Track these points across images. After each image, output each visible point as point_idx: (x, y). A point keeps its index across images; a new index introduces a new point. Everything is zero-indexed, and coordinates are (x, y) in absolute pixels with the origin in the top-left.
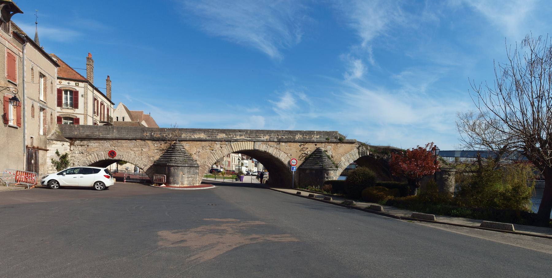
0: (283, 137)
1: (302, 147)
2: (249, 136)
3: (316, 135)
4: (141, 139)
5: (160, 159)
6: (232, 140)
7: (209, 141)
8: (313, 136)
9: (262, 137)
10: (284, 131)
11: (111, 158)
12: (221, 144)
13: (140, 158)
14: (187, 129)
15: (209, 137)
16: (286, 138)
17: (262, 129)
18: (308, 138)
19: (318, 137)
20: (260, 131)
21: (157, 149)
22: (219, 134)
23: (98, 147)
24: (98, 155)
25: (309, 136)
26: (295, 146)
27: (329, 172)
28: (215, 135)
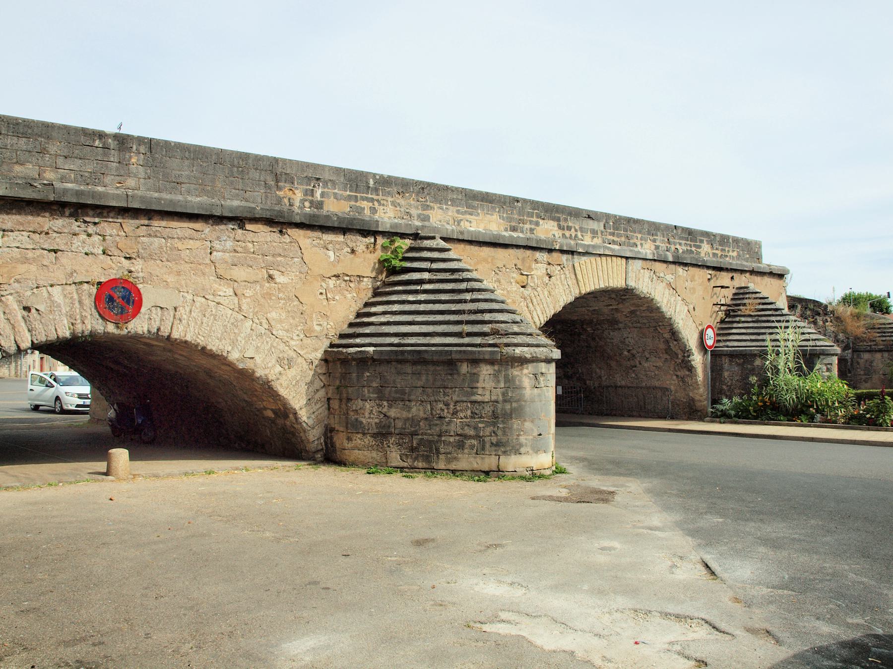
0: (678, 246)
1: (713, 283)
2: (611, 238)
4: (269, 222)
5: (351, 325)
6: (580, 250)
7: (518, 247)
9: (638, 244)
11: (111, 328)
12: (549, 264)
13: (264, 321)
14: (446, 188)
15: (514, 229)
17: (639, 218)
20: (636, 221)
21: (337, 276)
22: (541, 222)
23: (30, 254)
24: (27, 309)
25: (722, 250)
28: (531, 222)
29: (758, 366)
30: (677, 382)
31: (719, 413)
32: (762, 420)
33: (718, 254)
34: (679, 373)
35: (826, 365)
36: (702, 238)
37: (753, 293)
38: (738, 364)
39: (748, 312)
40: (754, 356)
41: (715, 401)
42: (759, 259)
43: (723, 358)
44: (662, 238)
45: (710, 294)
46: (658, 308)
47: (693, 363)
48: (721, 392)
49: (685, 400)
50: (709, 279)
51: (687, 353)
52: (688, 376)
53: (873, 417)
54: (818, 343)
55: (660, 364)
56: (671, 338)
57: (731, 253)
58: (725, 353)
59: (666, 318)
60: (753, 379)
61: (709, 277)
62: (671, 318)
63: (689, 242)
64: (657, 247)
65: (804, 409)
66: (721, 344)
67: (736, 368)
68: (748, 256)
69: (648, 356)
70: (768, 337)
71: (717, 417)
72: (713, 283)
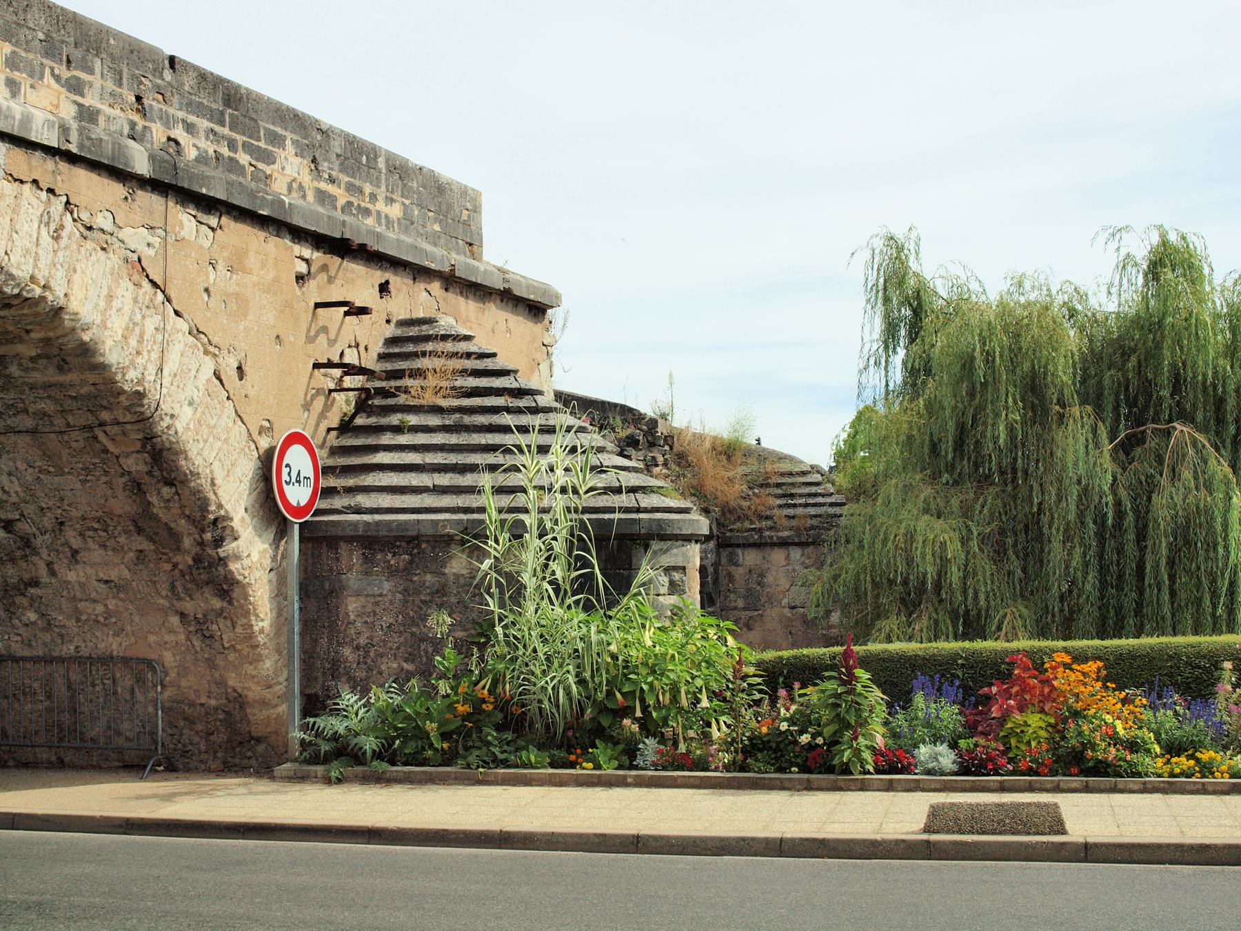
0: (179, 133)
1: (315, 291)
3: (383, 188)
10: (187, 66)
19: (395, 211)
25: (350, 188)
29: (457, 576)
30: (182, 637)
31: (325, 747)
32: (468, 766)
34: (188, 606)
35: (668, 570)
36: (279, 130)
37: (445, 338)
38: (392, 572)
39: (429, 399)
40: (443, 541)
41: (314, 704)
42: (473, 246)
43: (344, 549)
44: (110, 85)
45: (304, 326)
46: (86, 351)
47: (234, 567)
48: (335, 669)
49: (213, 702)
50: (300, 278)
51: (220, 529)
52: (220, 613)
53: (820, 741)
54: (646, 501)
55: (119, 572)
56: (150, 473)
57: (380, 206)
58: (349, 532)
59: (121, 392)
60: (441, 622)
61: (302, 268)
62: (140, 395)
63: (226, 131)
64: (88, 115)
65: (605, 723)
66: (338, 502)
67: (387, 586)
68: (437, 228)
69: (76, 543)
70: (486, 480)
71: (316, 759)
72: (315, 291)
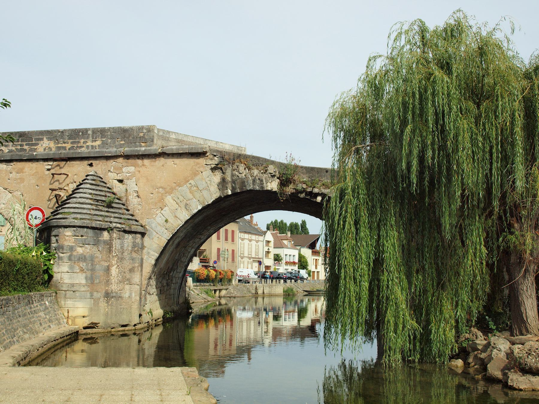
1: (53, 171)
3: (91, 138)
8: (82, 141)
16: (10, 151)
18: (69, 149)
19: (98, 143)
25: (72, 143)
26: (34, 171)
27: (59, 233)
33: (66, 147)
50: (49, 170)
57: (90, 143)
61: (49, 167)
63: (20, 143)
68: (123, 142)
